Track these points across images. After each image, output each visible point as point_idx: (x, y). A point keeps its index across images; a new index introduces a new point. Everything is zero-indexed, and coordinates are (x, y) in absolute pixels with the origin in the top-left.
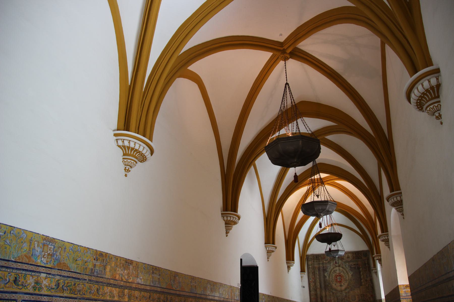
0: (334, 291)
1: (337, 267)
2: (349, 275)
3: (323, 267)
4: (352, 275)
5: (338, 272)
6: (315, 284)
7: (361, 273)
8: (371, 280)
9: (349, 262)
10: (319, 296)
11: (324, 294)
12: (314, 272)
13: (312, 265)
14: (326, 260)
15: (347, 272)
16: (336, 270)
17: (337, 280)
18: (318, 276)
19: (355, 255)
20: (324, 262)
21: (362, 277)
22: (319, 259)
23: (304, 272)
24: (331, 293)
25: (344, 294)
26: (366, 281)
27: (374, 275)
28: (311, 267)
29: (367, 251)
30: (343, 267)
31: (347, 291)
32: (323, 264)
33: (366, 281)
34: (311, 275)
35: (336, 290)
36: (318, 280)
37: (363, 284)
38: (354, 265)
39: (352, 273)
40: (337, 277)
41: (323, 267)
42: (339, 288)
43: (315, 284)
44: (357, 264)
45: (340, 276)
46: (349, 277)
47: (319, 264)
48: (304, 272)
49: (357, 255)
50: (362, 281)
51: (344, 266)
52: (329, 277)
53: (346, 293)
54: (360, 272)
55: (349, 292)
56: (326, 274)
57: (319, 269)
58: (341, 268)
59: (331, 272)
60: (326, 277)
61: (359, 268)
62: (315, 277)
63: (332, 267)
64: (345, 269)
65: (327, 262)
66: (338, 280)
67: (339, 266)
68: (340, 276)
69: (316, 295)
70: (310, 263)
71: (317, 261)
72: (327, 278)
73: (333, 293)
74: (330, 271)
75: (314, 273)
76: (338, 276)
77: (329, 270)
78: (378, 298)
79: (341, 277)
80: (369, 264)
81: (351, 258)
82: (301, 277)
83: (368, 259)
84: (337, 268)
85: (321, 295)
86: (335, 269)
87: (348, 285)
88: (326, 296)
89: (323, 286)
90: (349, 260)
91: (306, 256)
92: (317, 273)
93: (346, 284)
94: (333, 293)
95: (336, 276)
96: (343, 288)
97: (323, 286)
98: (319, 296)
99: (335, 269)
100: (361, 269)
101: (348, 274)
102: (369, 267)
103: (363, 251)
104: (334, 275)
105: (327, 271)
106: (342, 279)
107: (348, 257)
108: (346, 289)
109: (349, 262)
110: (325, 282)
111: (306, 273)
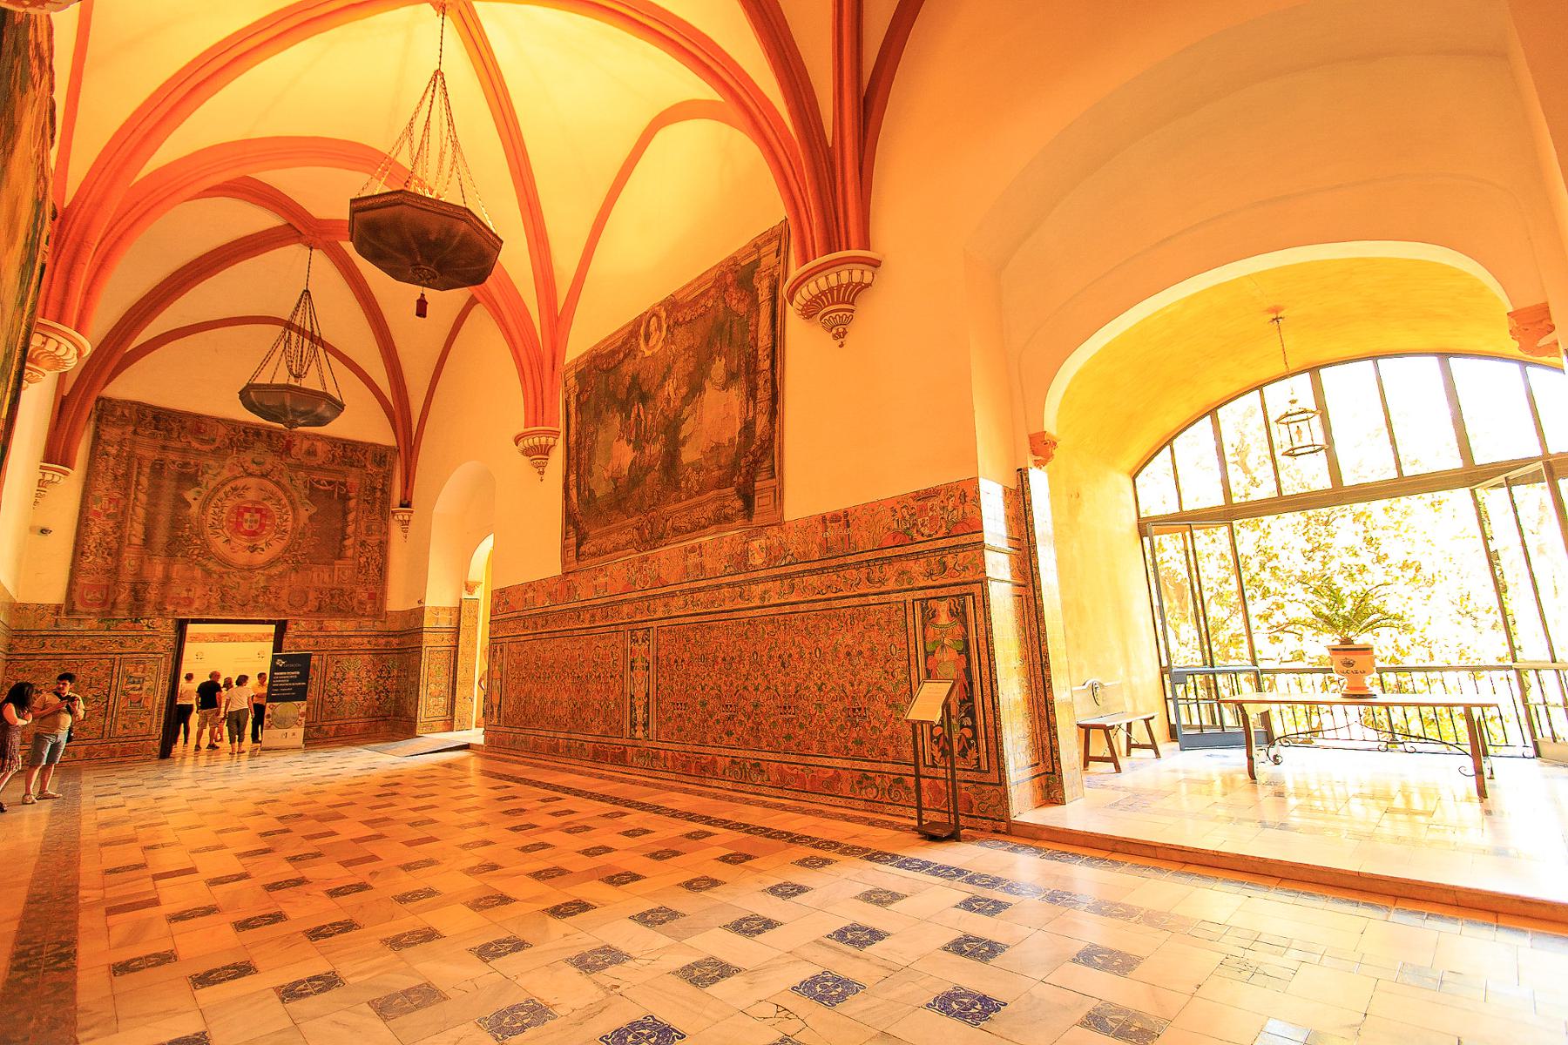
0: (212, 566)
1: (251, 475)
2: (294, 517)
3: (185, 465)
4: (310, 518)
5: (251, 495)
6: (119, 526)
7: (351, 517)
8: (383, 546)
9: (310, 469)
10: (127, 578)
11: (157, 570)
12: (127, 475)
13: (121, 444)
14: (203, 441)
15: (292, 503)
16: (246, 488)
17: (239, 524)
18: (142, 497)
19: (339, 452)
20: (195, 444)
21: (350, 529)
22: (170, 431)
23: (67, 461)
24: (198, 573)
25: (260, 579)
26: (363, 544)
27: (396, 531)
28: (113, 451)
29: (388, 448)
30: (278, 483)
31: (274, 571)
32: (184, 450)
33: (363, 544)
34: (103, 486)
35: (225, 562)
36: (140, 512)
37: (349, 553)
38: (330, 483)
39: (313, 510)
40: (240, 514)
41: (185, 465)
42: (242, 557)
43: (119, 526)
44: (344, 484)
45: (258, 511)
46: (295, 520)
47: (164, 448)
48: (67, 461)
49: (349, 451)
50: (348, 543)
51: (285, 481)
52: (204, 507)
53: (270, 577)
54: (345, 513)
55: (281, 576)
56: (189, 495)
57: (158, 469)
58: (270, 486)
59: (216, 490)
60: (189, 506)
61: (345, 499)
62: (126, 496)
63: (226, 474)
64: (285, 490)
65: (206, 448)
66: (246, 526)
67: (263, 476)
68: (258, 511)
69: (114, 572)
70: (112, 433)
71: (153, 436)
72: (194, 510)
73: (208, 573)
74: (212, 484)
75: (124, 482)
76: (248, 510)
77: (209, 481)
78: (396, 602)
79: (263, 516)
80: (386, 492)
81: (321, 458)
82: (42, 483)
83: (388, 477)
84: (252, 481)
85: (138, 574)
86: (240, 483)
87: (286, 550)
88: (167, 580)
89: (161, 537)
90: (316, 461)
91: (99, 399)
92: (144, 481)
93: (277, 547)
94: (208, 573)
95: (240, 511)
96: (261, 558)
97: (161, 537)
98: (127, 578)
99: (240, 483)
100: (352, 503)
101: (294, 510)
102: (386, 502)
103: (376, 445)
104: (229, 504)
105: (199, 485)
106: (262, 526)
107: (311, 453)
108: (271, 563)
109: (310, 469)
110: (176, 524)
111: (77, 473)
